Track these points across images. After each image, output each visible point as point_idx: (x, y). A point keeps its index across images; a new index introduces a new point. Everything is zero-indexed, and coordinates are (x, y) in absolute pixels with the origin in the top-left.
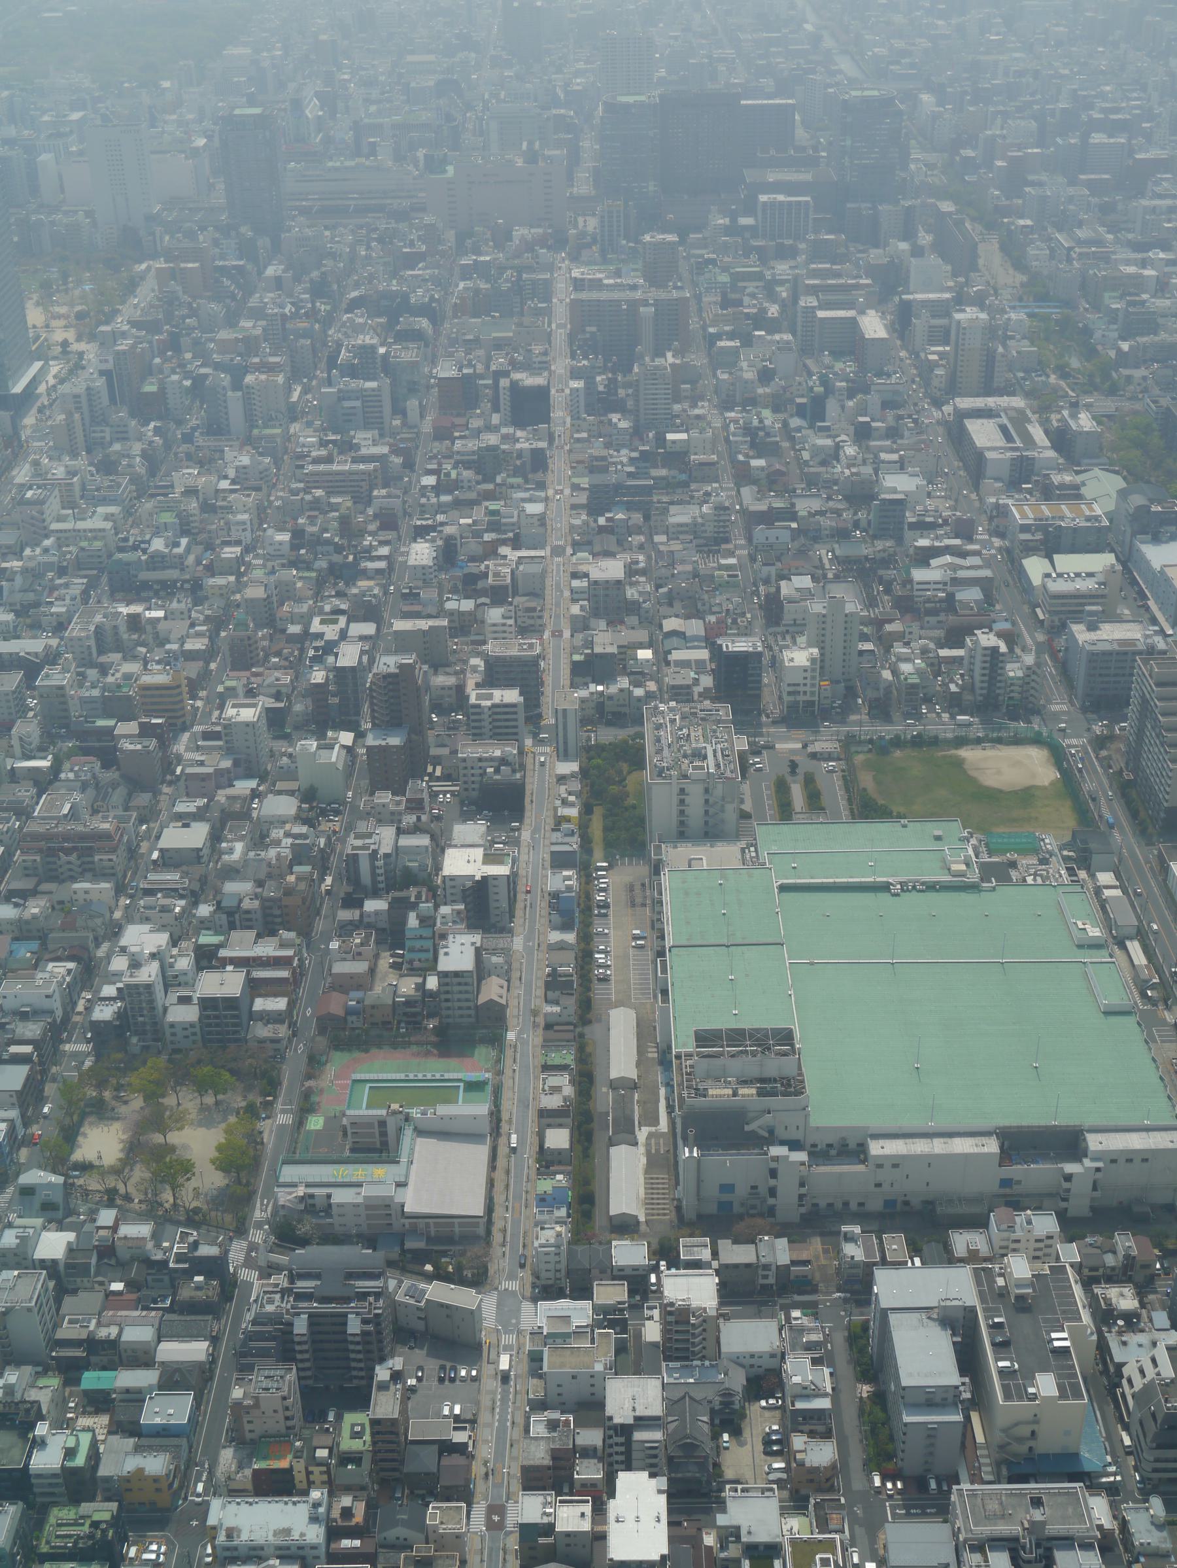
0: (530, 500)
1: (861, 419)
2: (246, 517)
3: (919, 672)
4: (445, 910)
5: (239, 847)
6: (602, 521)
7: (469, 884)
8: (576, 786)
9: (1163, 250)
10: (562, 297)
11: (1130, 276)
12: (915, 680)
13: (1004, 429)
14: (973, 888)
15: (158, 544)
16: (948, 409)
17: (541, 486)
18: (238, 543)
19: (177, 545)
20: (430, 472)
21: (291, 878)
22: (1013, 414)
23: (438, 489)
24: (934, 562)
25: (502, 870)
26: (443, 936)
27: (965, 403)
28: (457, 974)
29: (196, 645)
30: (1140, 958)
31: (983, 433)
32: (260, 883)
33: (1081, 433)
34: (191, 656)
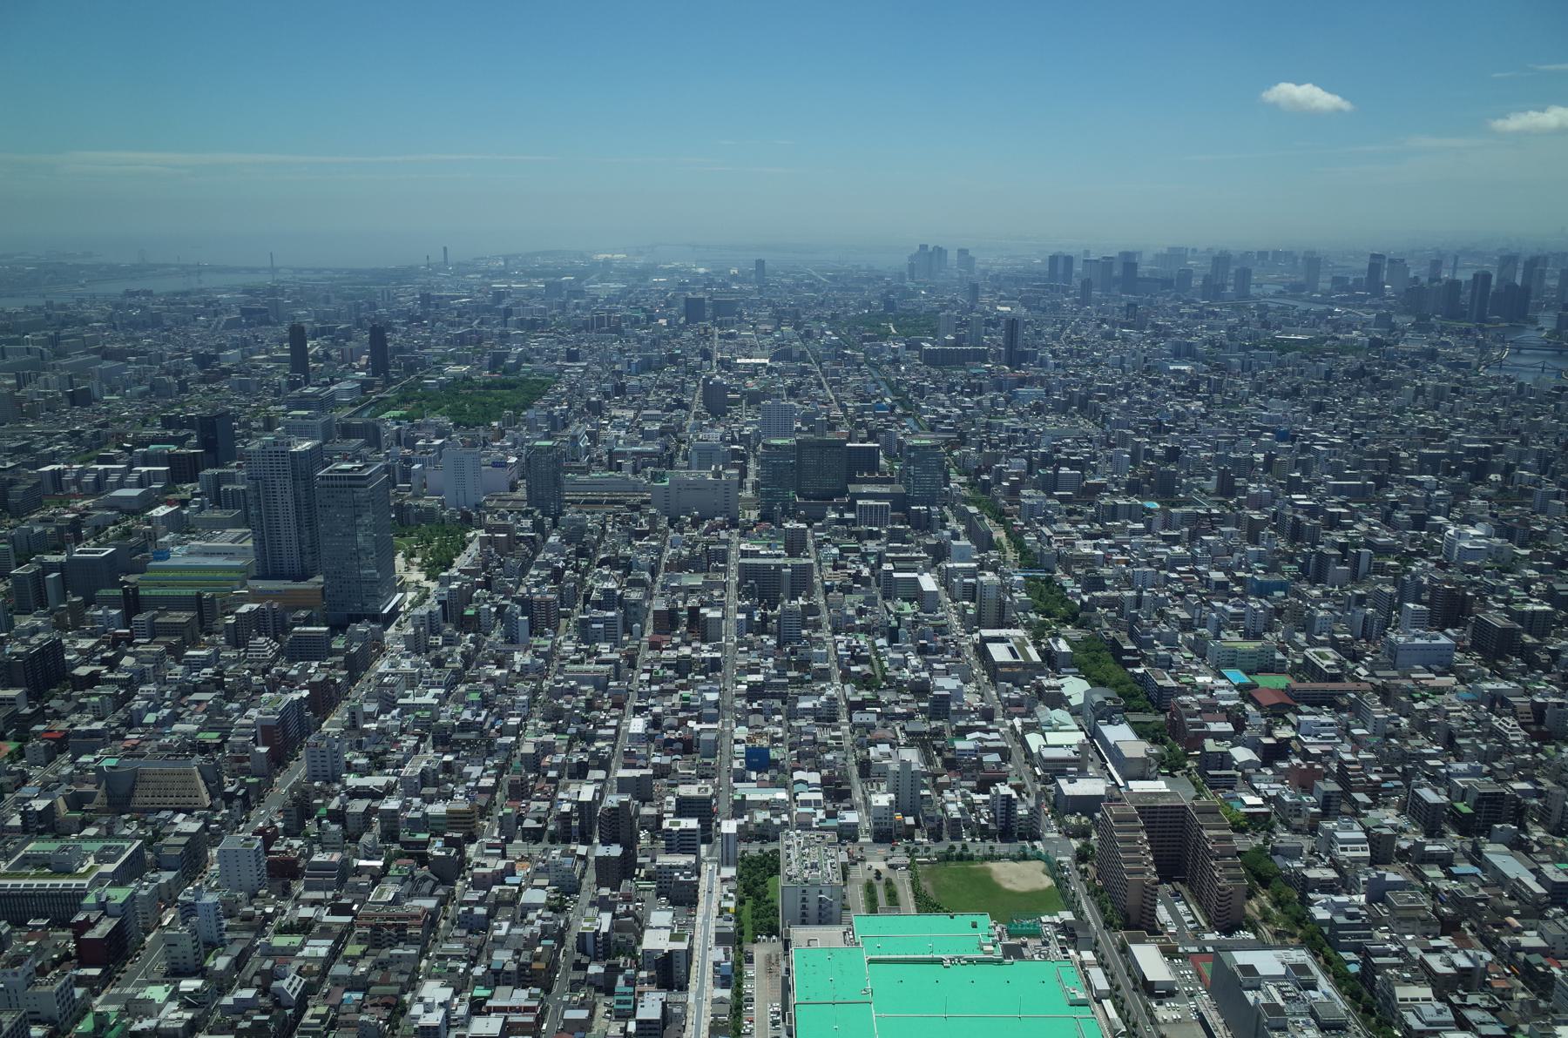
0: (710, 691)
2: (525, 697)
3: (960, 810)
4: (643, 974)
5: (506, 925)
6: (755, 705)
7: (660, 955)
8: (733, 886)
10: (735, 560)
11: (1087, 555)
12: (957, 815)
13: (1011, 649)
14: (999, 962)
15: (467, 715)
16: (976, 636)
17: (717, 682)
18: (518, 715)
19: (480, 715)
20: (645, 671)
21: (539, 949)
22: (1017, 640)
23: (650, 682)
24: (969, 736)
25: (683, 946)
26: (641, 993)
27: (987, 633)
28: (649, 1022)
29: (487, 782)
30: (1113, 1013)
31: (999, 653)
32: (518, 952)
33: (1061, 653)
34: (483, 790)
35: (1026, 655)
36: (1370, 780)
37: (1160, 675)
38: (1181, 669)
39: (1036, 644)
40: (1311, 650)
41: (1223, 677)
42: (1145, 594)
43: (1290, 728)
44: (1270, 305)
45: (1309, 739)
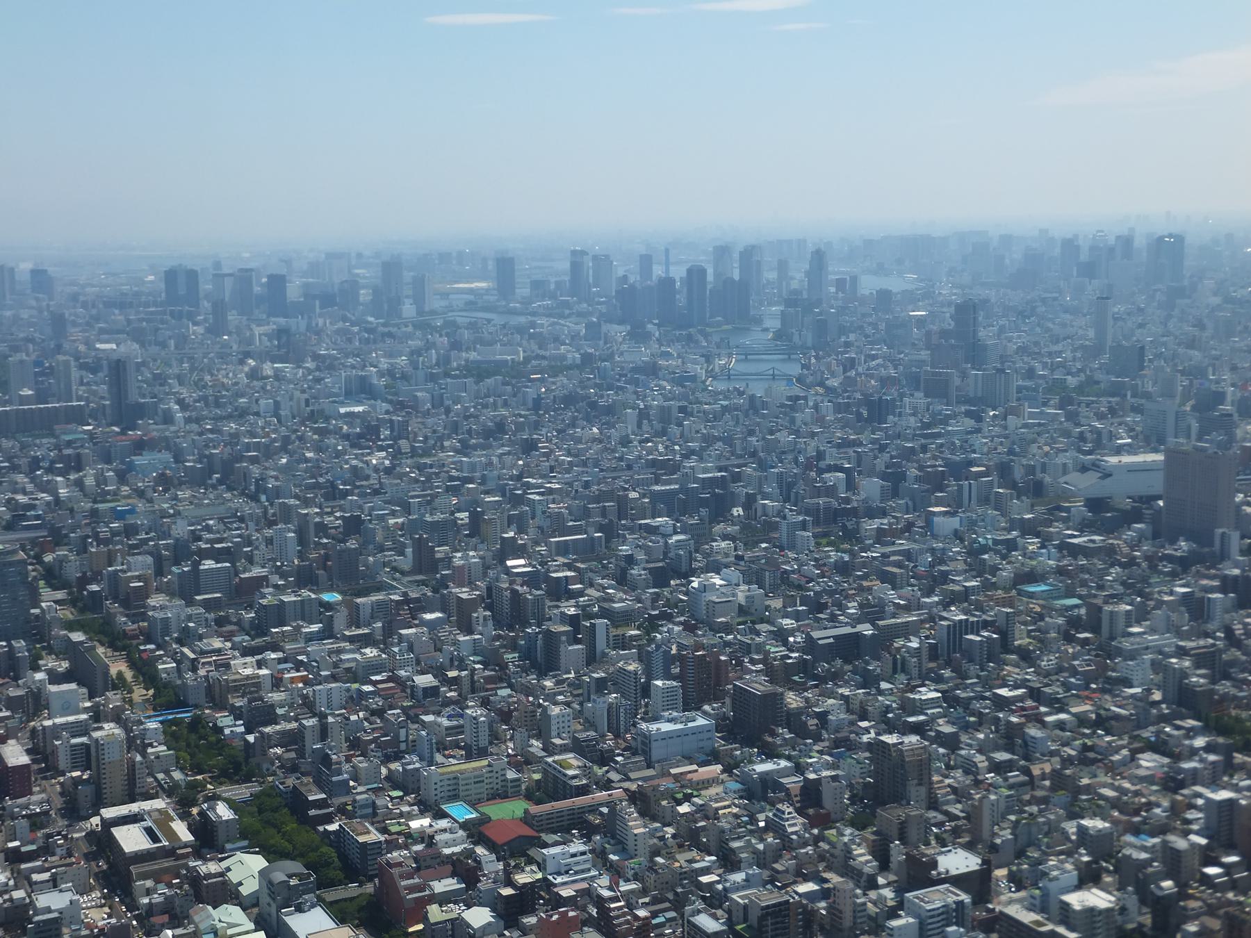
1: (11, 845)
9: (274, 651)
11: (248, 677)
13: (149, 832)
16: (95, 820)
22: (156, 815)
31: (131, 839)
35: (172, 835)
36: (636, 918)
37: (360, 828)
38: (390, 815)
39: (184, 816)
40: (550, 760)
41: (443, 815)
42: (330, 719)
43: (534, 868)
44: (459, 320)
45: (559, 880)
